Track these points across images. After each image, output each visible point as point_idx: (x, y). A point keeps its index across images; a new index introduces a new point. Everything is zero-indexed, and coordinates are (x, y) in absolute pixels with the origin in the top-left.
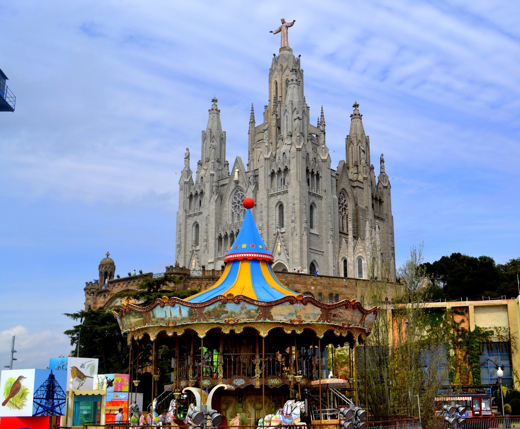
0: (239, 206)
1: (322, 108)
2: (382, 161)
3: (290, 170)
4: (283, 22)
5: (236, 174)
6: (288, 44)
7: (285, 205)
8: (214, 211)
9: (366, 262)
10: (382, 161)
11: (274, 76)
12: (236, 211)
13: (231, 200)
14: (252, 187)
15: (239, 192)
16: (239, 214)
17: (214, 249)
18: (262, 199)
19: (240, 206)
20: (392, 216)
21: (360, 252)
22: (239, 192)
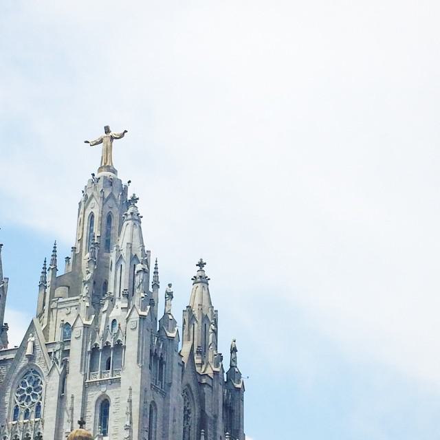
0: (29, 396)
2: (234, 350)
3: (125, 347)
4: (107, 130)
5: (30, 345)
6: (112, 164)
10: (234, 350)
11: (90, 206)
12: (23, 404)
13: (16, 386)
14: (60, 369)
15: (31, 374)
19: (31, 397)
22: (31, 374)
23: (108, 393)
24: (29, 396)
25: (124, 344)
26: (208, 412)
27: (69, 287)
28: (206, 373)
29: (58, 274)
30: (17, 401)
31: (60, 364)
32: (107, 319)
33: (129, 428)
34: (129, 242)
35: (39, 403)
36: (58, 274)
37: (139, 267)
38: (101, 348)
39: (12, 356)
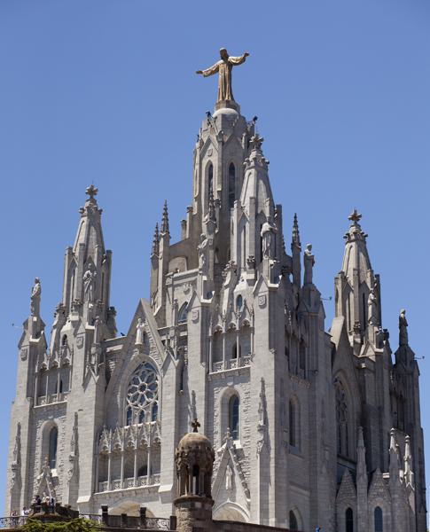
0: (143, 396)
1: (295, 217)
2: (403, 323)
6: (232, 99)
7: (242, 397)
8: (94, 402)
9: (389, 514)
10: (403, 323)
11: (207, 154)
12: (137, 405)
13: (127, 382)
14: (175, 362)
17: (91, 476)
18: (196, 382)
20: (422, 429)
21: (379, 495)
23: (237, 387)
24: (138, 394)
25: (251, 326)
26: (370, 400)
27: (187, 258)
28: (367, 355)
29: (172, 242)
32: (231, 294)
34: (252, 195)
35: (156, 403)
36: (172, 242)
37: (266, 227)
38: (224, 331)
39: (119, 347)
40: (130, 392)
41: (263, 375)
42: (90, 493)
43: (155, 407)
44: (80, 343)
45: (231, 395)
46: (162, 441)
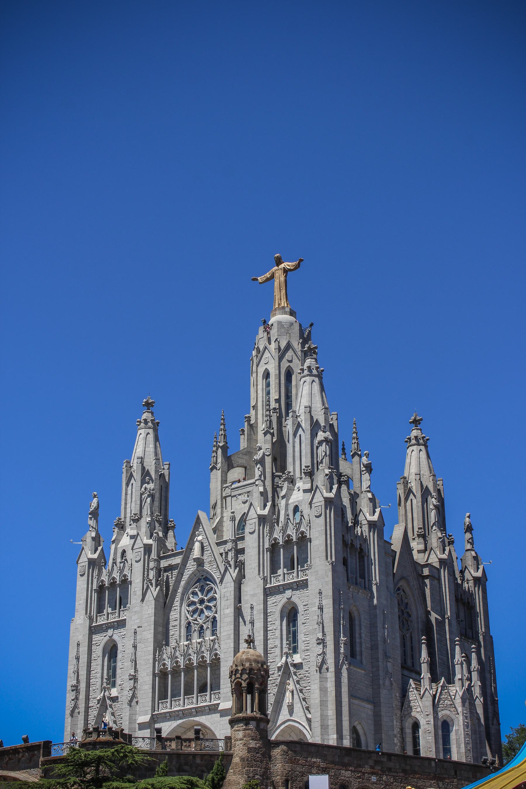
8: (153, 618)
11: (263, 361)
12: (196, 620)
14: (234, 573)
16: (202, 627)
18: (254, 595)
19: (205, 610)
20: (491, 637)
23: (295, 599)
25: (308, 537)
27: (246, 468)
28: (429, 562)
30: (188, 616)
31: (233, 567)
33: (322, 642)
35: (214, 618)
37: (321, 435)
39: (177, 560)
40: (189, 606)
41: (320, 587)
42: (150, 712)
43: (214, 621)
44: (138, 559)
45: (290, 608)
46: (222, 656)
